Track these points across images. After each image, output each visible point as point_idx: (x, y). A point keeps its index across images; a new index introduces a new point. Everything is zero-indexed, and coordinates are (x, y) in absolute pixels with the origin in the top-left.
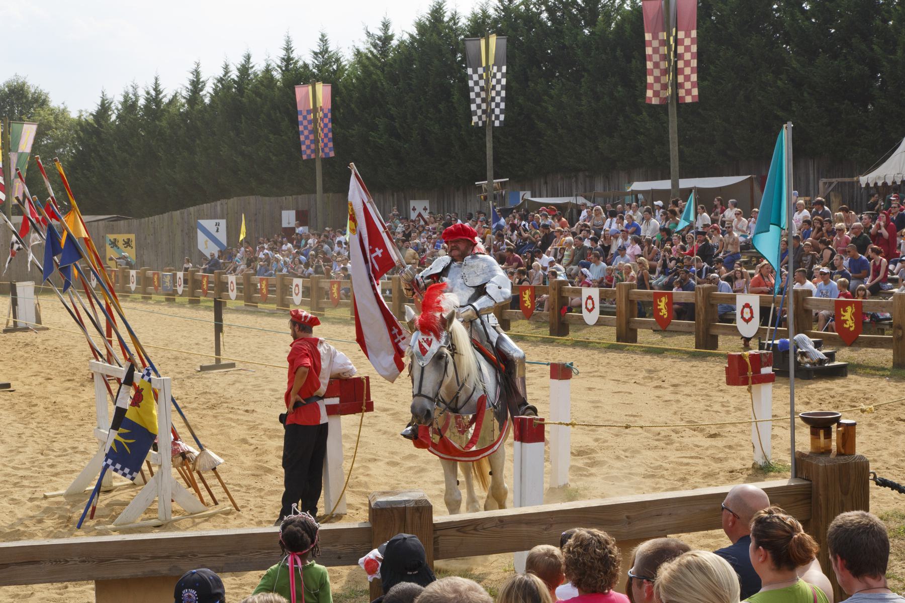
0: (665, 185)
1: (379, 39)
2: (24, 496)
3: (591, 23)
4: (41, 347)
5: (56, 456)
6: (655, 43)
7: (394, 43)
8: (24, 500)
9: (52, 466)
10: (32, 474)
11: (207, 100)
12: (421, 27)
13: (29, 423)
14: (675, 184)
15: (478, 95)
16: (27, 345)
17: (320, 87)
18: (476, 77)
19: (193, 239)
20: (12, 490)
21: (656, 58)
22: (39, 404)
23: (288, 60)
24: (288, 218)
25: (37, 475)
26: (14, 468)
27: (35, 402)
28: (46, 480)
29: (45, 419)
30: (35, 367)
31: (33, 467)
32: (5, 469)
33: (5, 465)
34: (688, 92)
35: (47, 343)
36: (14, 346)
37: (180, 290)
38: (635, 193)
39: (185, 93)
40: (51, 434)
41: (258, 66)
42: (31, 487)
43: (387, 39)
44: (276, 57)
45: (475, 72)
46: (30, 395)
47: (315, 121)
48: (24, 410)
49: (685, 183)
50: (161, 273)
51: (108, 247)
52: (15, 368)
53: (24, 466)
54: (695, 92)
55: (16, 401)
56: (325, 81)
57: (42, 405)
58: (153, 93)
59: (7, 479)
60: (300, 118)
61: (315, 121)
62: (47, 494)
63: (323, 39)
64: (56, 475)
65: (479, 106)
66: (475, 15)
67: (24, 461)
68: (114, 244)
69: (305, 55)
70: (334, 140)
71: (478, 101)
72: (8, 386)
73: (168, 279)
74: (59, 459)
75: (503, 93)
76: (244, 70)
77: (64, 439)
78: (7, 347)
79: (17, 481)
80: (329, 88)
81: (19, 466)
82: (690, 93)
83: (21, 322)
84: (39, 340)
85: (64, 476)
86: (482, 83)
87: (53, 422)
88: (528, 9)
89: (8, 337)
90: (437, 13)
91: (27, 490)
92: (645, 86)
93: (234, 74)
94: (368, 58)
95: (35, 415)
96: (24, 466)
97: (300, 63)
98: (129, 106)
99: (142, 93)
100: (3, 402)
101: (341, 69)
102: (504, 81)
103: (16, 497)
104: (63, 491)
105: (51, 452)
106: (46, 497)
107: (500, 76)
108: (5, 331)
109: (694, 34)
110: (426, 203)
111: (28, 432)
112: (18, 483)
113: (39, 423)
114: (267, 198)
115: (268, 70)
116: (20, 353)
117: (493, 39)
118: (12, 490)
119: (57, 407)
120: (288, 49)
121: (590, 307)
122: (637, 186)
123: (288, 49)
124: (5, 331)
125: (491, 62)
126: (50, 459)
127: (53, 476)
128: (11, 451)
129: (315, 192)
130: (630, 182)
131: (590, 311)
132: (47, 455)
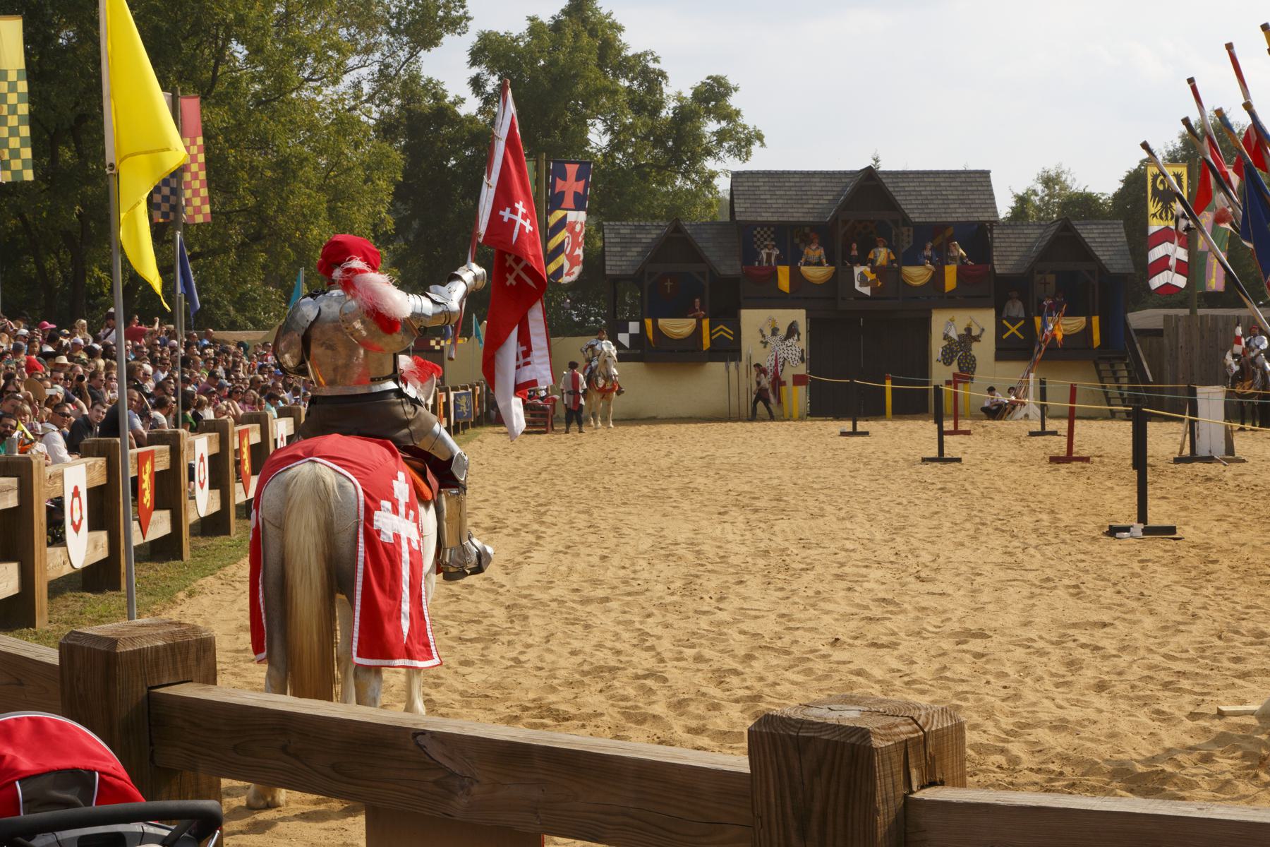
2: (1180, 708)
4: (1232, 484)
5: (1244, 643)
8: (1180, 715)
9: (1237, 660)
10: (1197, 671)
13: (1201, 587)
16: (1209, 479)
20: (1160, 694)
22: (1221, 560)
25: (1207, 672)
26: (1166, 656)
27: (1214, 557)
28: (1224, 682)
29: (1230, 583)
30: (1220, 509)
31: (1202, 657)
32: (1150, 656)
33: (1150, 651)
35: (1240, 479)
36: (1188, 480)
40: (1239, 607)
42: (1195, 693)
46: (1207, 547)
48: (1195, 568)
52: (1184, 509)
53: (1184, 655)
55: (1183, 554)
57: (1225, 563)
59: (1151, 673)
62: (1224, 708)
64: (1244, 675)
67: (1186, 646)
72: (1171, 530)
74: (1251, 650)
77: (1261, 617)
78: (1177, 480)
79: (1171, 679)
81: (1176, 655)
83: (1202, 451)
84: (1228, 474)
85: (1259, 679)
87: (1244, 589)
89: (1179, 469)
91: (1188, 698)
95: (1213, 575)
96: (1184, 655)
100: (1161, 554)
103: (1166, 709)
104: (1255, 707)
105: (1236, 636)
106: (1221, 714)
108: (1177, 461)
111: (1198, 601)
112: (1171, 682)
113: (1218, 589)
116: (1197, 488)
118: (1160, 694)
119: (1251, 566)
124: (1177, 461)
126: (1234, 647)
127: (1239, 677)
128: (1165, 628)
132: (1229, 640)
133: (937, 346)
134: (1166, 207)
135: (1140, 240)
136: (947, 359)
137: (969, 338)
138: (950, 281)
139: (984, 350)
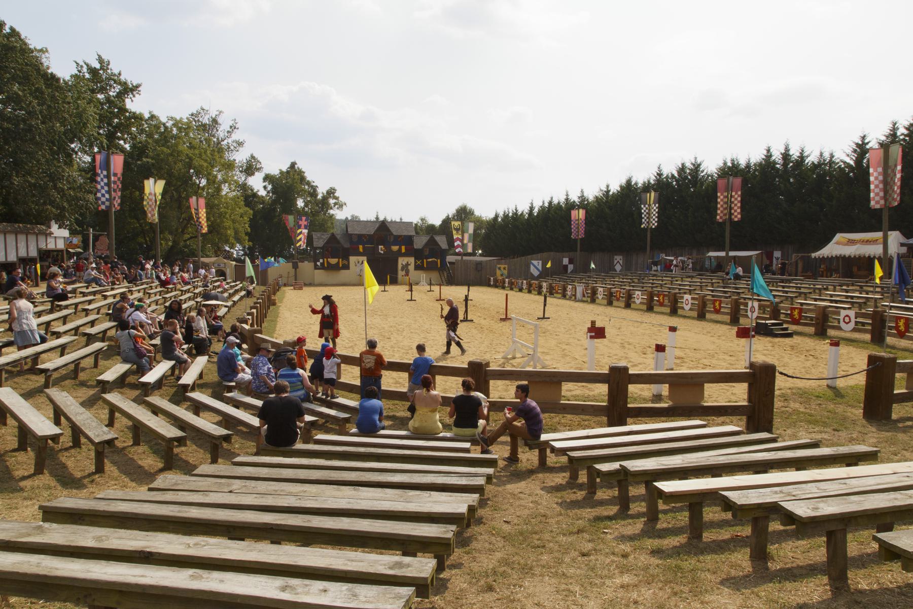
0: (723, 254)
1: (605, 192)
3: (694, 186)
6: (722, 197)
7: (611, 193)
11: (535, 214)
12: (621, 187)
14: (727, 254)
15: (645, 216)
17: (581, 211)
18: (644, 209)
19: (529, 268)
21: (721, 203)
23: (567, 199)
24: (566, 261)
34: (736, 217)
37: (524, 287)
38: (710, 257)
39: (527, 211)
41: (555, 201)
43: (608, 191)
44: (562, 199)
45: (645, 206)
47: (578, 224)
49: (732, 254)
50: (518, 281)
51: (497, 270)
54: (739, 216)
56: (583, 209)
58: (515, 211)
60: (572, 223)
61: (578, 224)
63: (582, 191)
65: (645, 220)
66: (644, 182)
68: (500, 268)
69: (574, 197)
70: (585, 231)
71: (645, 218)
73: (520, 283)
75: (657, 215)
76: (550, 203)
80: (584, 211)
82: (737, 216)
86: (647, 211)
88: (667, 180)
90: (629, 182)
92: (717, 214)
93: (546, 205)
94: (600, 199)
97: (572, 201)
98: (506, 216)
99: (510, 211)
101: (589, 203)
102: (657, 210)
107: (655, 208)
109: (739, 193)
110: (621, 257)
114: (558, 253)
115: (559, 203)
117: (653, 194)
120: (567, 195)
121: (687, 303)
122: (711, 254)
123: (567, 195)
125: (652, 202)
129: (576, 251)
130: (708, 252)
131: (687, 305)
133: (400, 266)
134: (457, 233)
135: (451, 241)
136: (402, 270)
137: (408, 264)
138: (403, 250)
139: (411, 268)
